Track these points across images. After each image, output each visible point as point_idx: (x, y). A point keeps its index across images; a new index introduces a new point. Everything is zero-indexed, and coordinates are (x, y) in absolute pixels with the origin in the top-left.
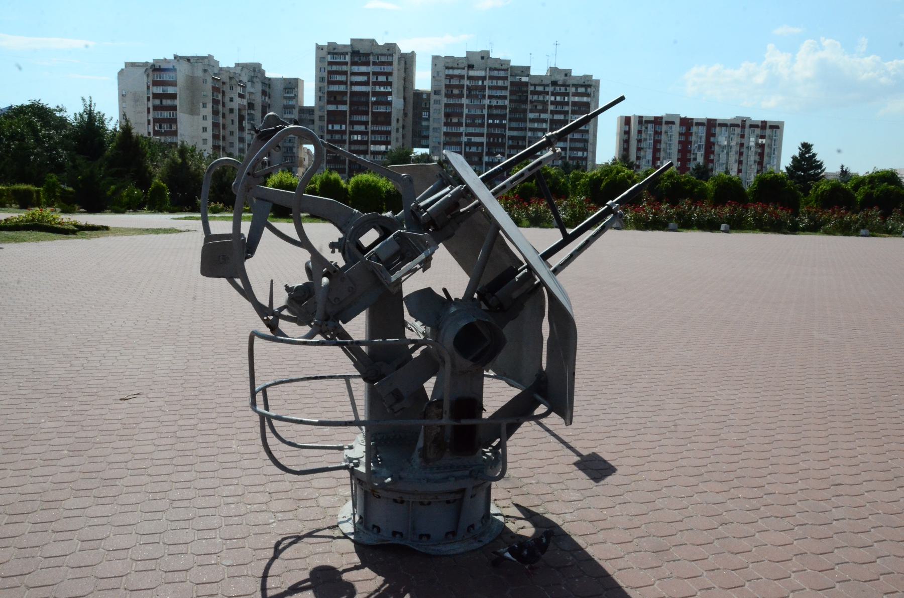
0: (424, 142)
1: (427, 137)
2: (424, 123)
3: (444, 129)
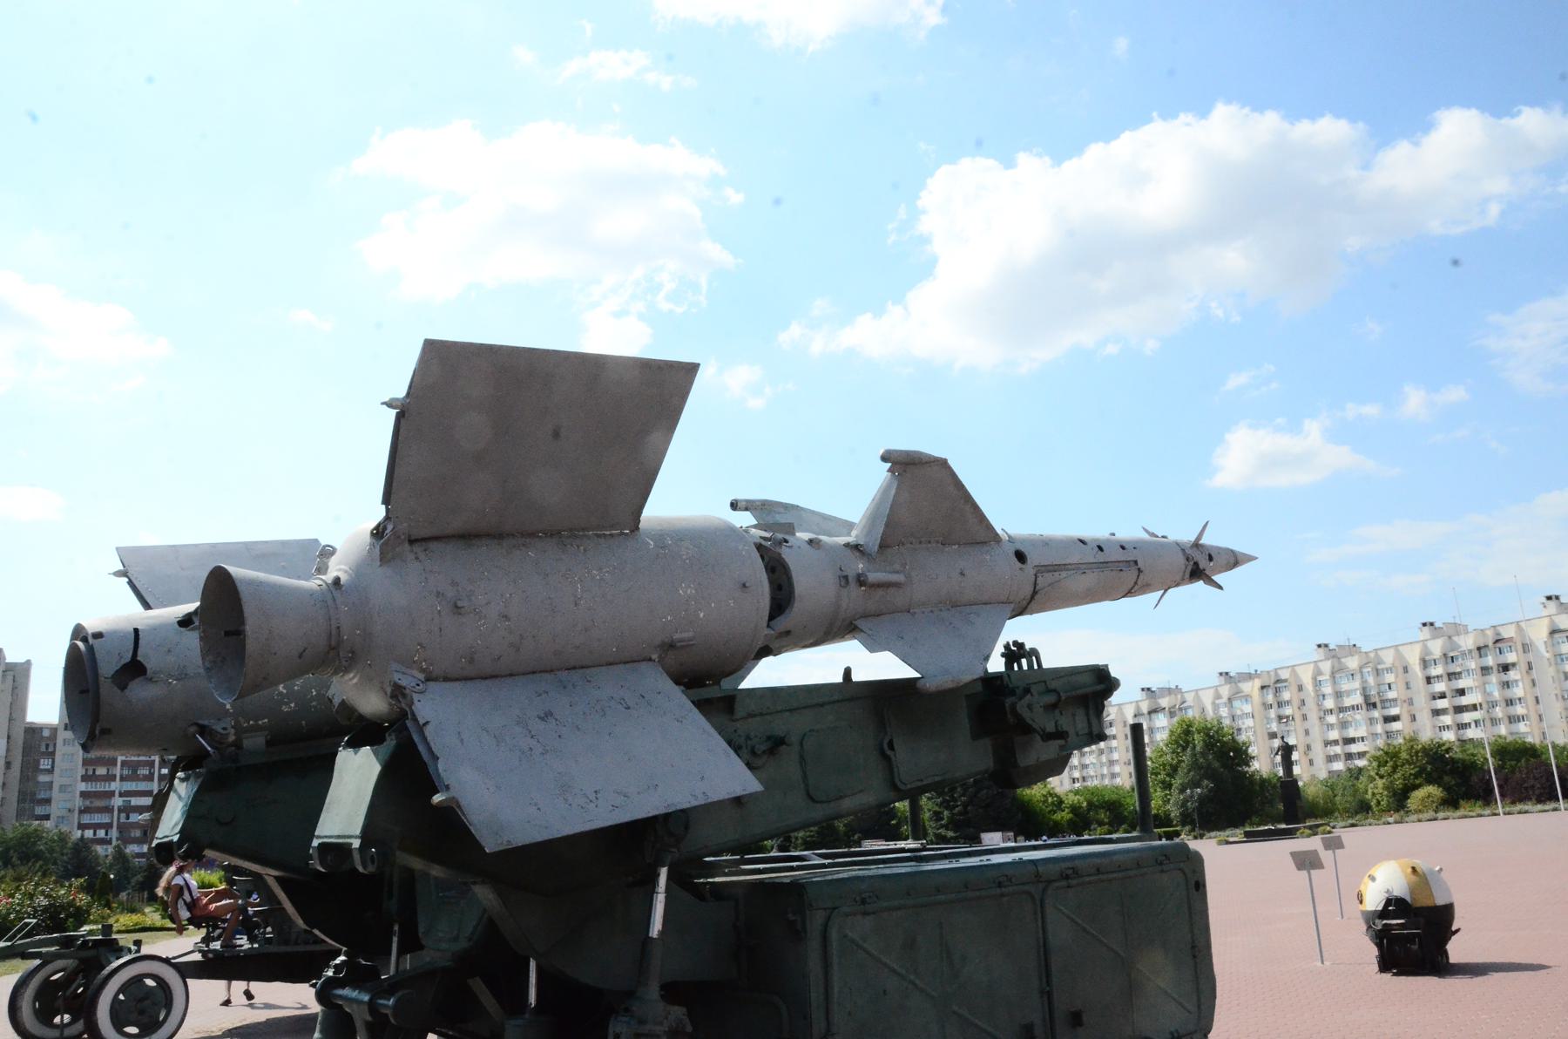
0: (39, 810)
1: (48, 801)
2: (43, 778)
3: (83, 787)
